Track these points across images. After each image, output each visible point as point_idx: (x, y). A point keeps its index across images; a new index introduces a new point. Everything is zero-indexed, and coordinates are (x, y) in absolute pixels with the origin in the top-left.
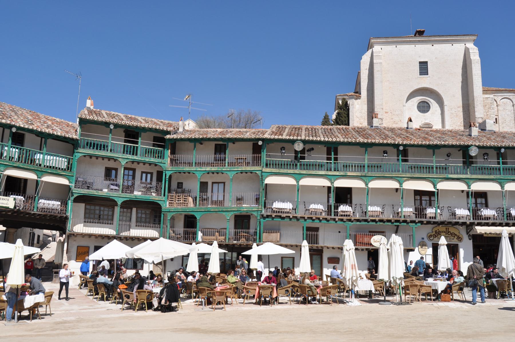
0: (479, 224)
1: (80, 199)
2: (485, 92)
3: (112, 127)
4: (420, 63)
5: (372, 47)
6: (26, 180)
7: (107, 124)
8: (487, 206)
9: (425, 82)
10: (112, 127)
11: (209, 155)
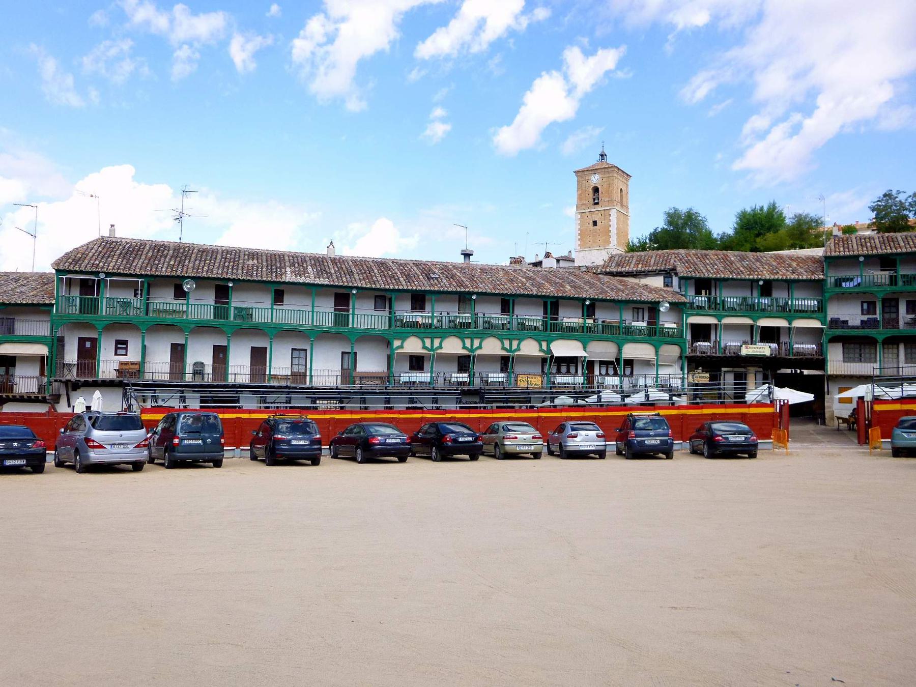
1: (834, 340)
3: (862, 259)
6: (778, 328)
10: (862, 259)
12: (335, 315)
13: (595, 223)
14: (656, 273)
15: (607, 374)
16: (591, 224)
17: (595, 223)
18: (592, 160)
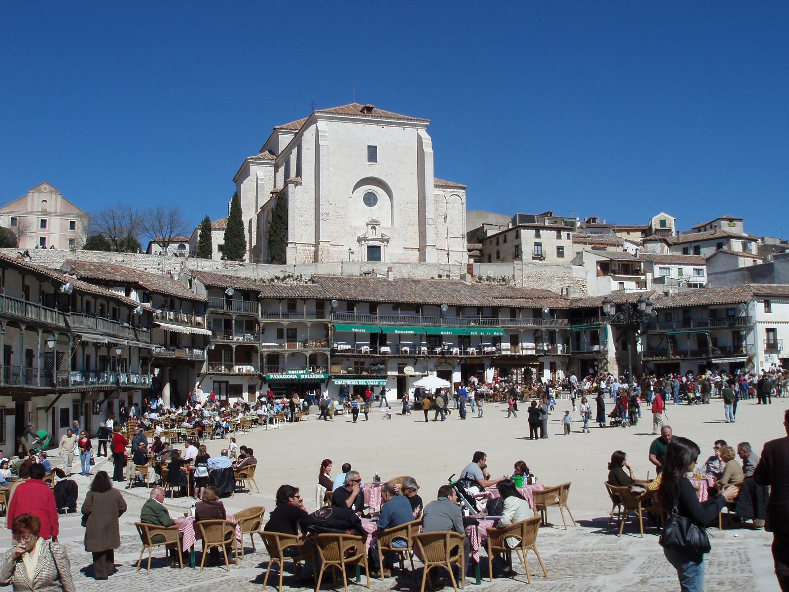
2: (436, 186)
5: (316, 122)
8: (470, 347)
11: (282, 308)
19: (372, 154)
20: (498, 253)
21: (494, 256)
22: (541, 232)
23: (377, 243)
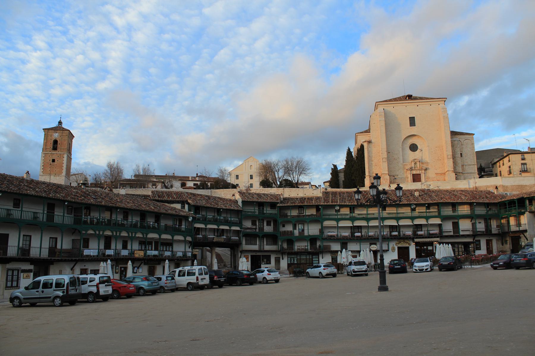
0: (417, 238)
4: (410, 118)
7: (254, 202)
9: (413, 130)
12: (74, 218)
13: (54, 161)
14: (178, 202)
15: (166, 250)
16: (51, 161)
17: (54, 161)
18: (55, 124)
19: (412, 121)
20: (500, 172)
21: (499, 174)
22: (526, 156)
23: (418, 172)
